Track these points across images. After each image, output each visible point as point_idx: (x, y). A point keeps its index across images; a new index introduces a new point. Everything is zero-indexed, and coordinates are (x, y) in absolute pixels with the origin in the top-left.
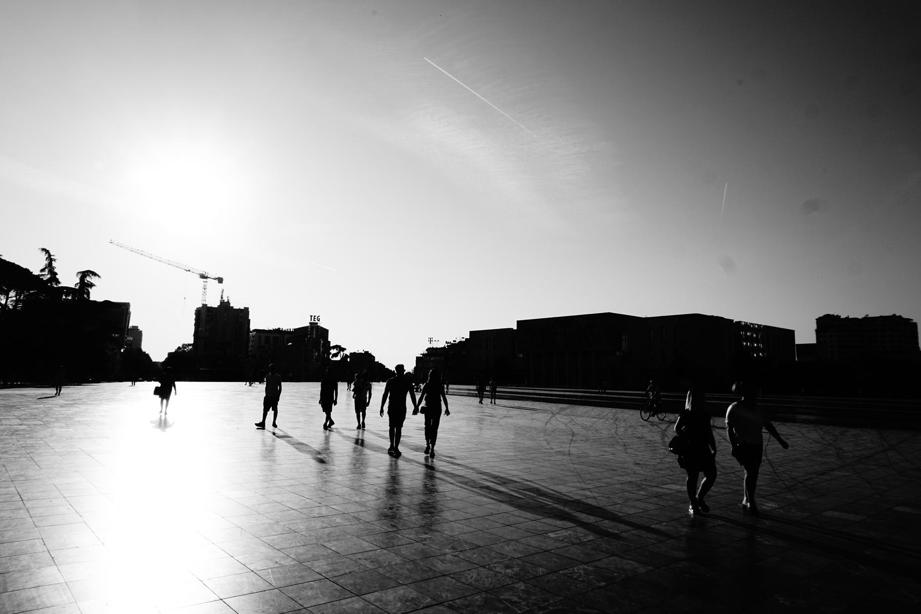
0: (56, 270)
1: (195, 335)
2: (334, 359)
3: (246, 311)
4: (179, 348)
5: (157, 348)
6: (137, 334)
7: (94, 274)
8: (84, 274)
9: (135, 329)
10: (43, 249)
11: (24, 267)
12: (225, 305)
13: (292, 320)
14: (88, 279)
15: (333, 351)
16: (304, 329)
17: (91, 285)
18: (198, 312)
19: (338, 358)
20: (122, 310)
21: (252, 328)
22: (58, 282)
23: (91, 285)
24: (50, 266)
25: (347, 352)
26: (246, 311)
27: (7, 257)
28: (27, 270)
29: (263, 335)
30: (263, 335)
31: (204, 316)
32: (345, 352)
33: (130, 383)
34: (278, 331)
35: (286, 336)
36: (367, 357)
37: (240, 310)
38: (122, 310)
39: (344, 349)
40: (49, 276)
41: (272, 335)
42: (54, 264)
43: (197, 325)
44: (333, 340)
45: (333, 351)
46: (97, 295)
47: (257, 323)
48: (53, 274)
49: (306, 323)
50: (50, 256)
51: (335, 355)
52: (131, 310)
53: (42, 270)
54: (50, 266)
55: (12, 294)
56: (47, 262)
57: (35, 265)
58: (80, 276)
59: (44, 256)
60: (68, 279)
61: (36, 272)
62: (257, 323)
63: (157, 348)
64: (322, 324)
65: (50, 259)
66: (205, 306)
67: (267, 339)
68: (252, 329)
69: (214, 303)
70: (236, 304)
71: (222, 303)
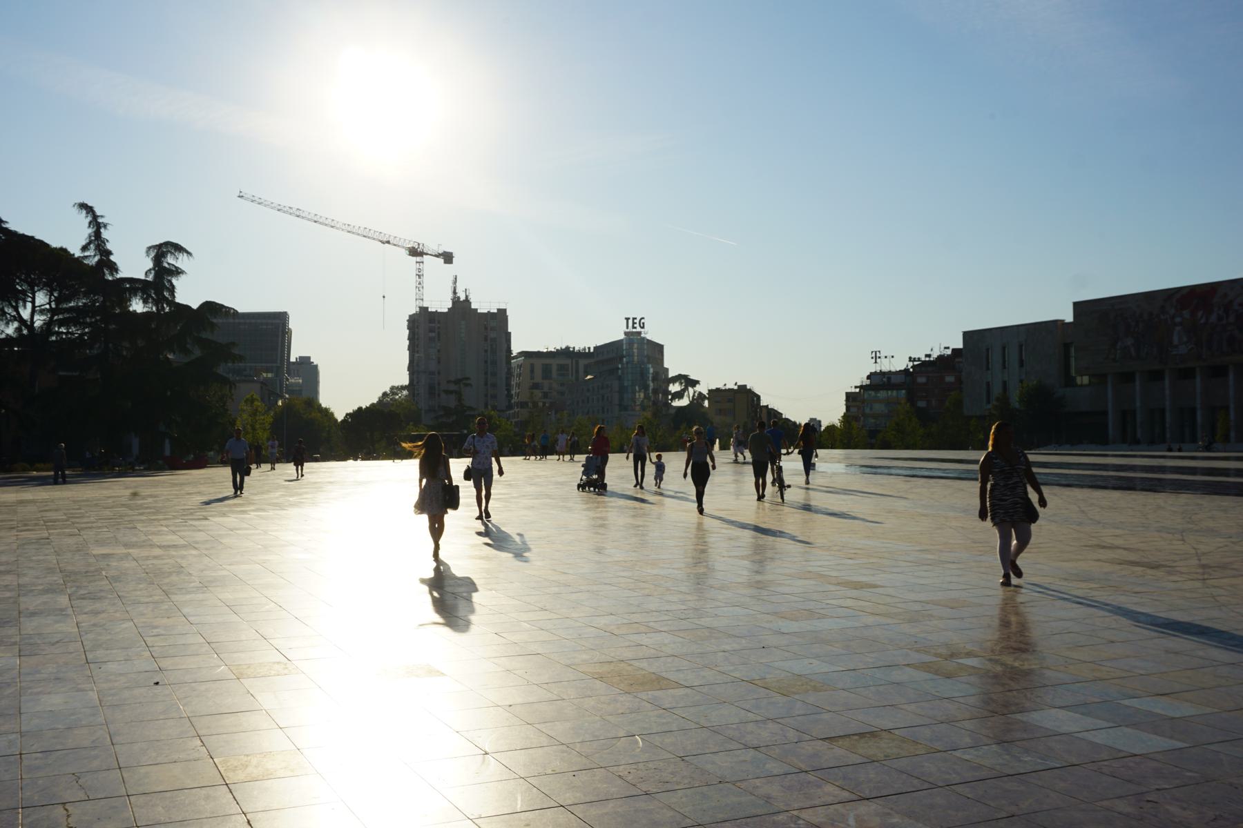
0: (109, 246)
1: (412, 368)
2: (677, 403)
3: (501, 316)
4: (385, 394)
5: (342, 395)
6: (308, 369)
7: (178, 248)
8: (162, 251)
9: (305, 362)
10: (83, 206)
11: (55, 243)
12: (461, 307)
13: (591, 330)
14: (170, 259)
15: (675, 388)
17: (177, 272)
18: (413, 322)
19: (684, 402)
20: (274, 328)
21: (516, 348)
22: (113, 268)
23: (177, 272)
24: (97, 240)
25: (703, 389)
26: (501, 316)
27: (19, 224)
28: (63, 251)
29: (538, 363)
31: (427, 331)
32: (698, 388)
33: (269, 466)
34: (566, 353)
35: (582, 362)
36: (745, 396)
37: (489, 315)
38: (274, 328)
39: (694, 383)
40: (96, 259)
41: (554, 362)
42: (105, 234)
43: (412, 348)
44: (674, 364)
45: (675, 388)
46: (189, 293)
47: (527, 337)
49: (616, 333)
50: (95, 217)
51: (679, 395)
52: (292, 324)
53: (84, 248)
54: (97, 240)
56: (90, 231)
57: (70, 236)
58: (153, 254)
59: (83, 219)
60: (133, 264)
61: (77, 253)
62: (527, 337)
63: (342, 395)
64: (651, 334)
65: (97, 225)
66: (424, 310)
67: (547, 371)
69: (440, 303)
70: (483, 304)
71: (456, 301)
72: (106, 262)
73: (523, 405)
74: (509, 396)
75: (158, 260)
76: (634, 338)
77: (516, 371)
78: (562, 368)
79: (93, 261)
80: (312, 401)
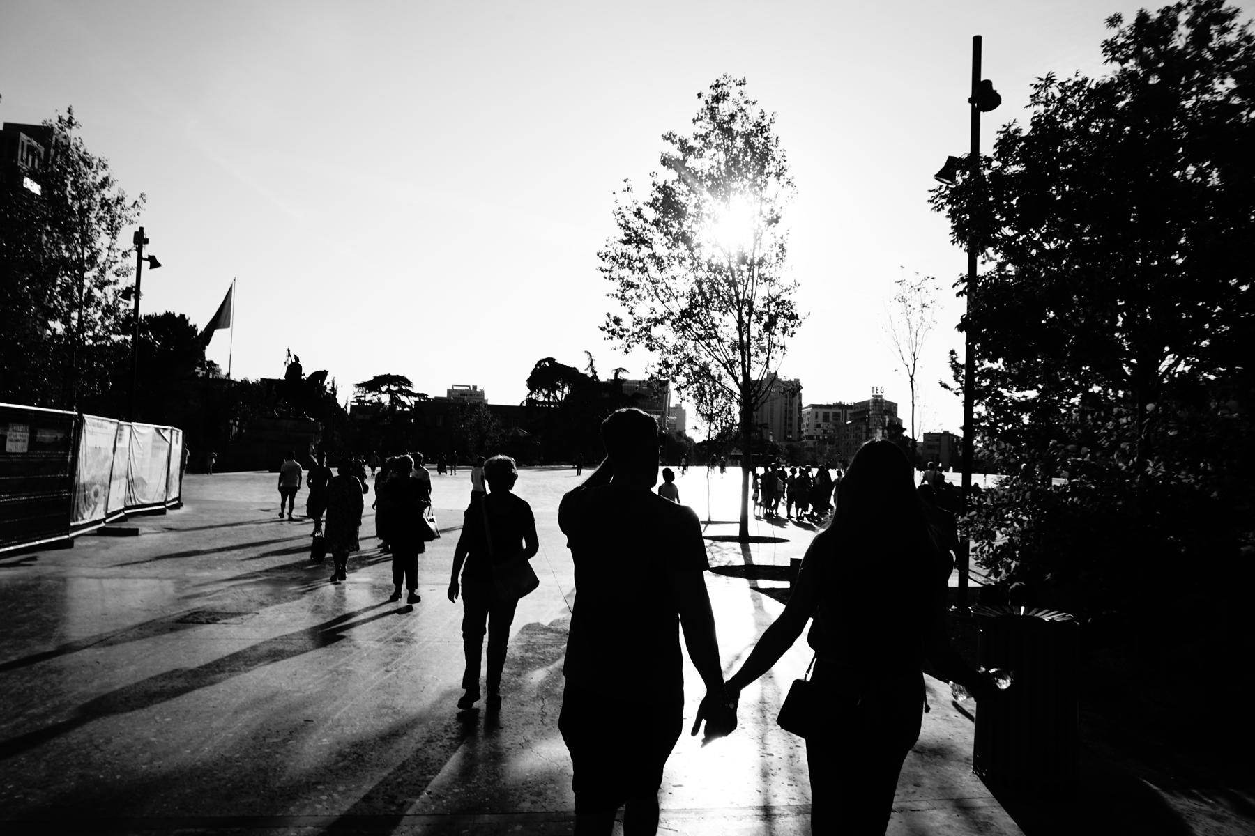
16: (867, 403)
29: (821, 412)
30: (821, 412)
34: (840, 406)
35: (849, 411)
41: (831, 411)
47: (809, 398)
48: (594, 372)
55: (566, 390)
61: (582, 371)
67: (826, 417)
68: (804, 404)
70: (785, 375)
72: (595, 376)
73: (810, 437)
74: (800, 432)
75: (616, 375)
76: (878, 401)
77: (805, 418)
78: (836, 415)
79: (590, 375)
80: (681, 434)
